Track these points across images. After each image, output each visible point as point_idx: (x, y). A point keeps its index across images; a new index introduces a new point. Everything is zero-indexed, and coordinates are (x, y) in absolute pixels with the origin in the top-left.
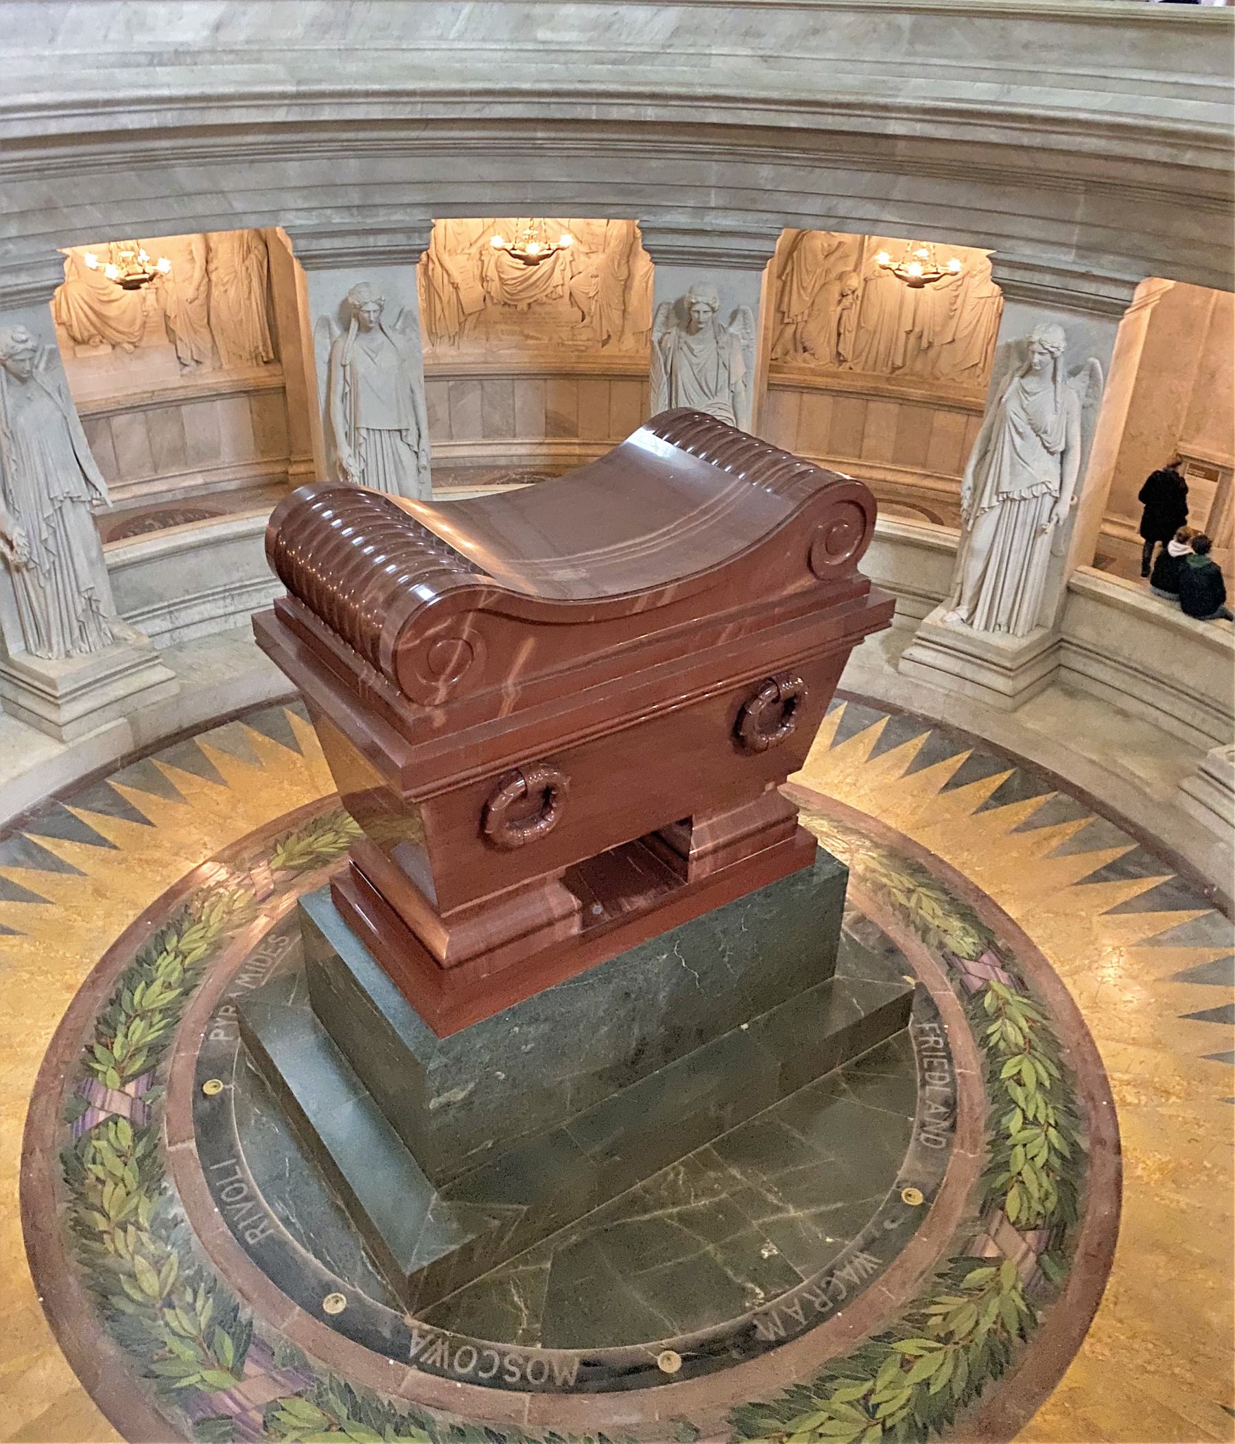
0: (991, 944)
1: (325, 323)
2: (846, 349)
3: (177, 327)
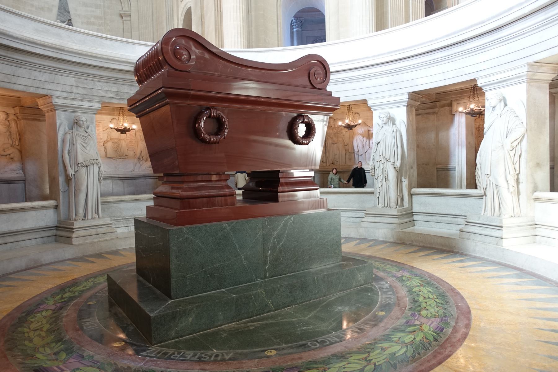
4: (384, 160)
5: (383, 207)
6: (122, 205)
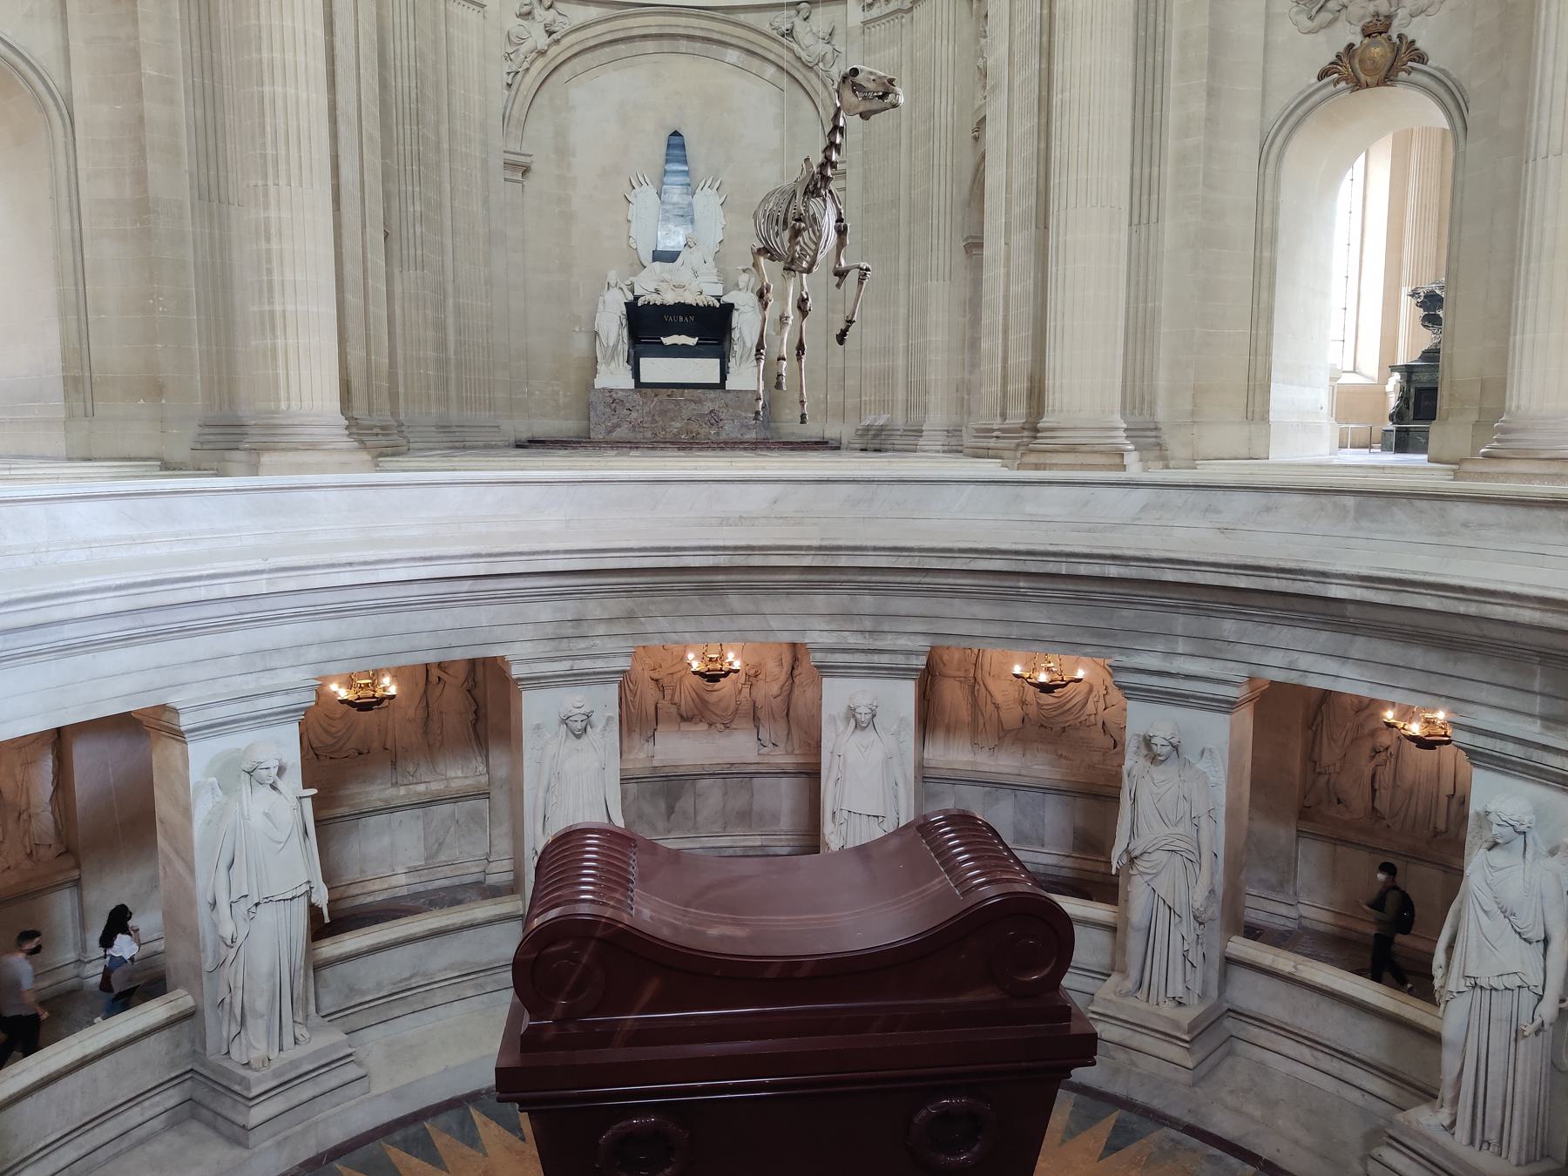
1: (833, 719)
2: (1383, 804)
3: (762, 714)
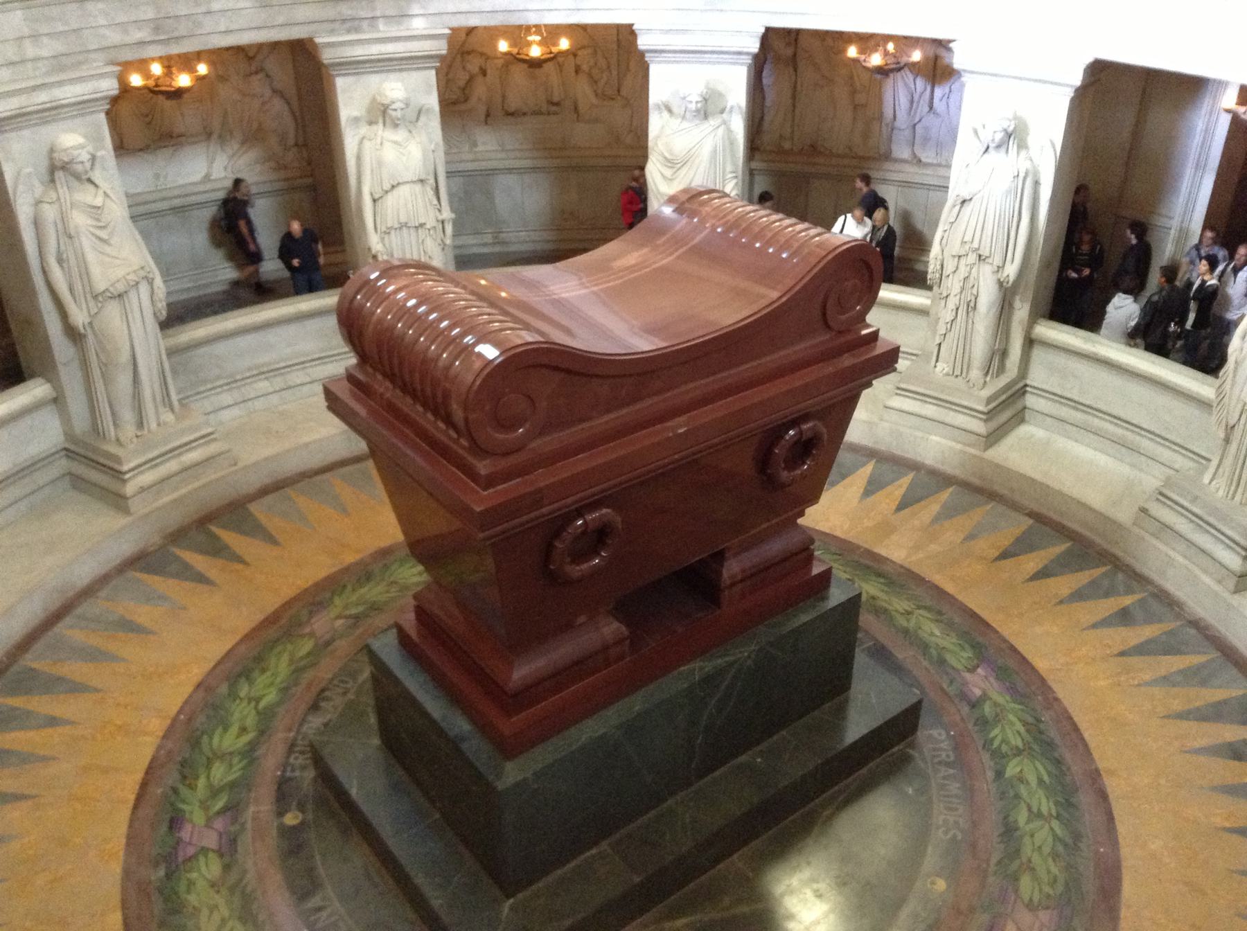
0: (168, 876)
4: (972, 258)
5: (947, 374)
6: (220, 348)
